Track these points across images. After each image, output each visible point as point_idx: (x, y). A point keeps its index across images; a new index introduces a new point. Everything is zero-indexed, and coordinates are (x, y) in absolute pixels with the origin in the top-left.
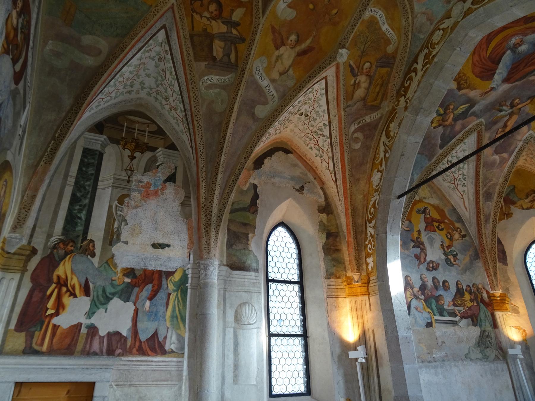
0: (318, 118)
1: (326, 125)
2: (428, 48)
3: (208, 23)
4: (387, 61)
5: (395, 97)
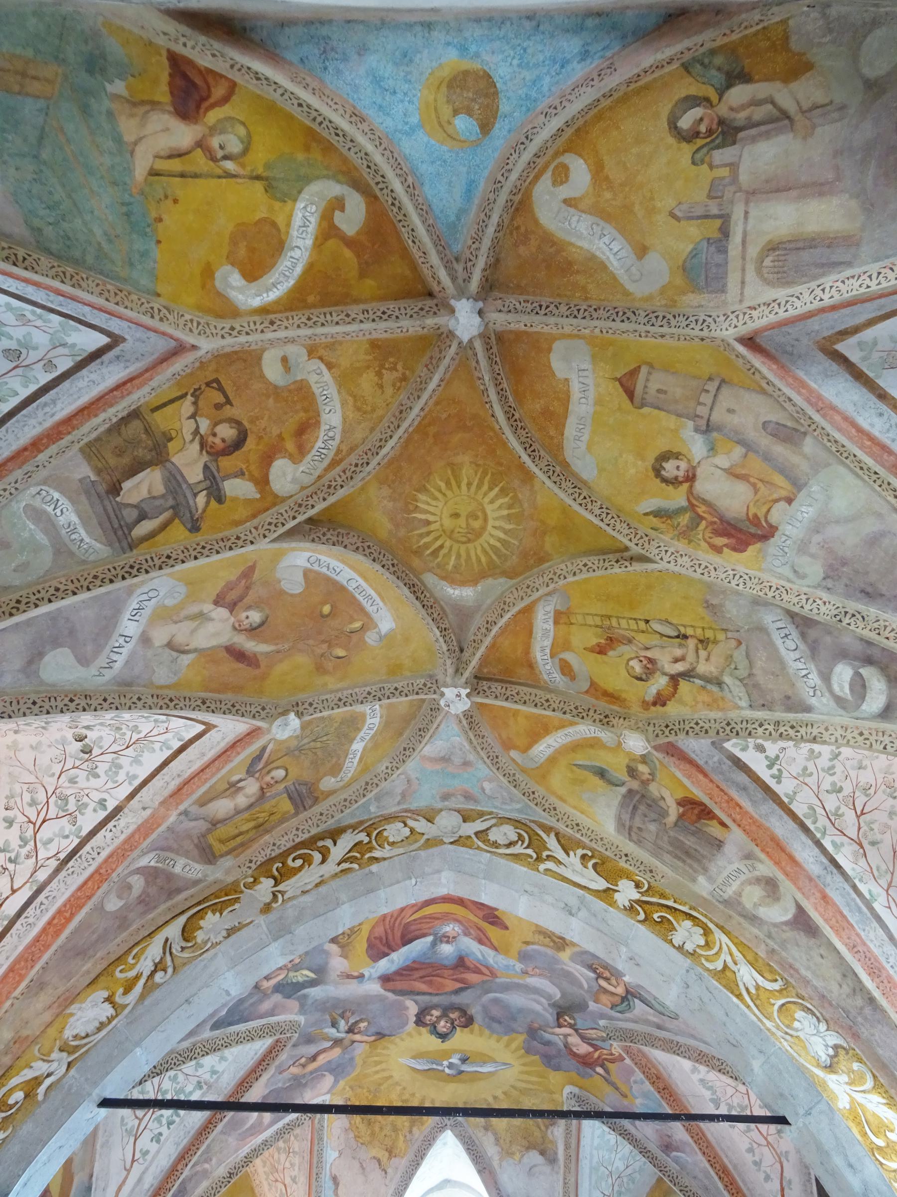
0: (103, 778)
1: (105, 808)
2: (368, 835)
3: (188, 437)
4: (303, 797)
5: (254, 866)
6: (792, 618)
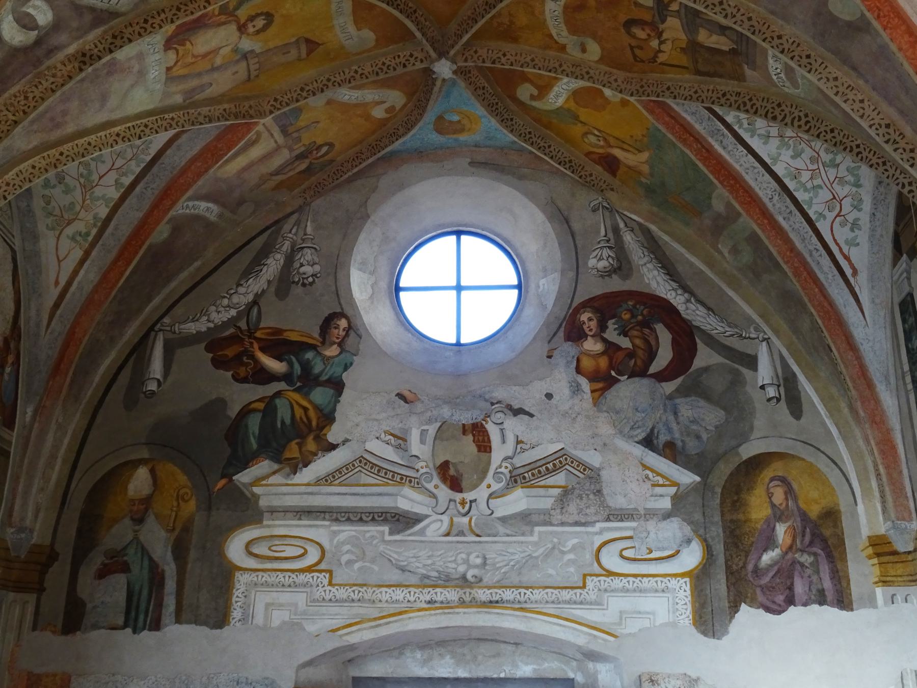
3: (669, 43)
6: (111, 13)
